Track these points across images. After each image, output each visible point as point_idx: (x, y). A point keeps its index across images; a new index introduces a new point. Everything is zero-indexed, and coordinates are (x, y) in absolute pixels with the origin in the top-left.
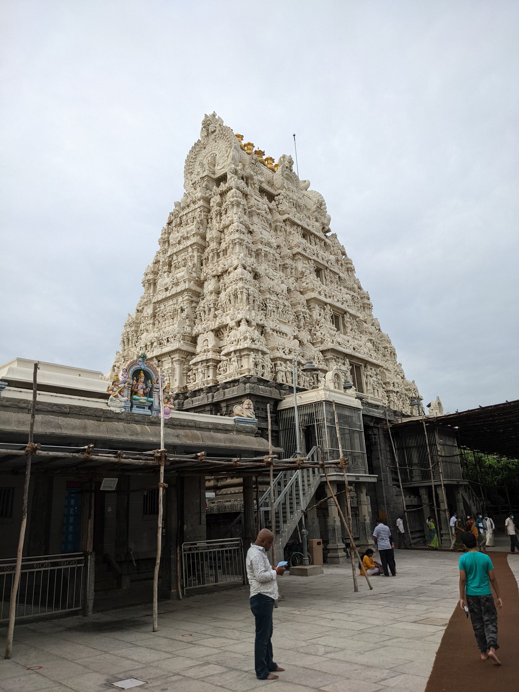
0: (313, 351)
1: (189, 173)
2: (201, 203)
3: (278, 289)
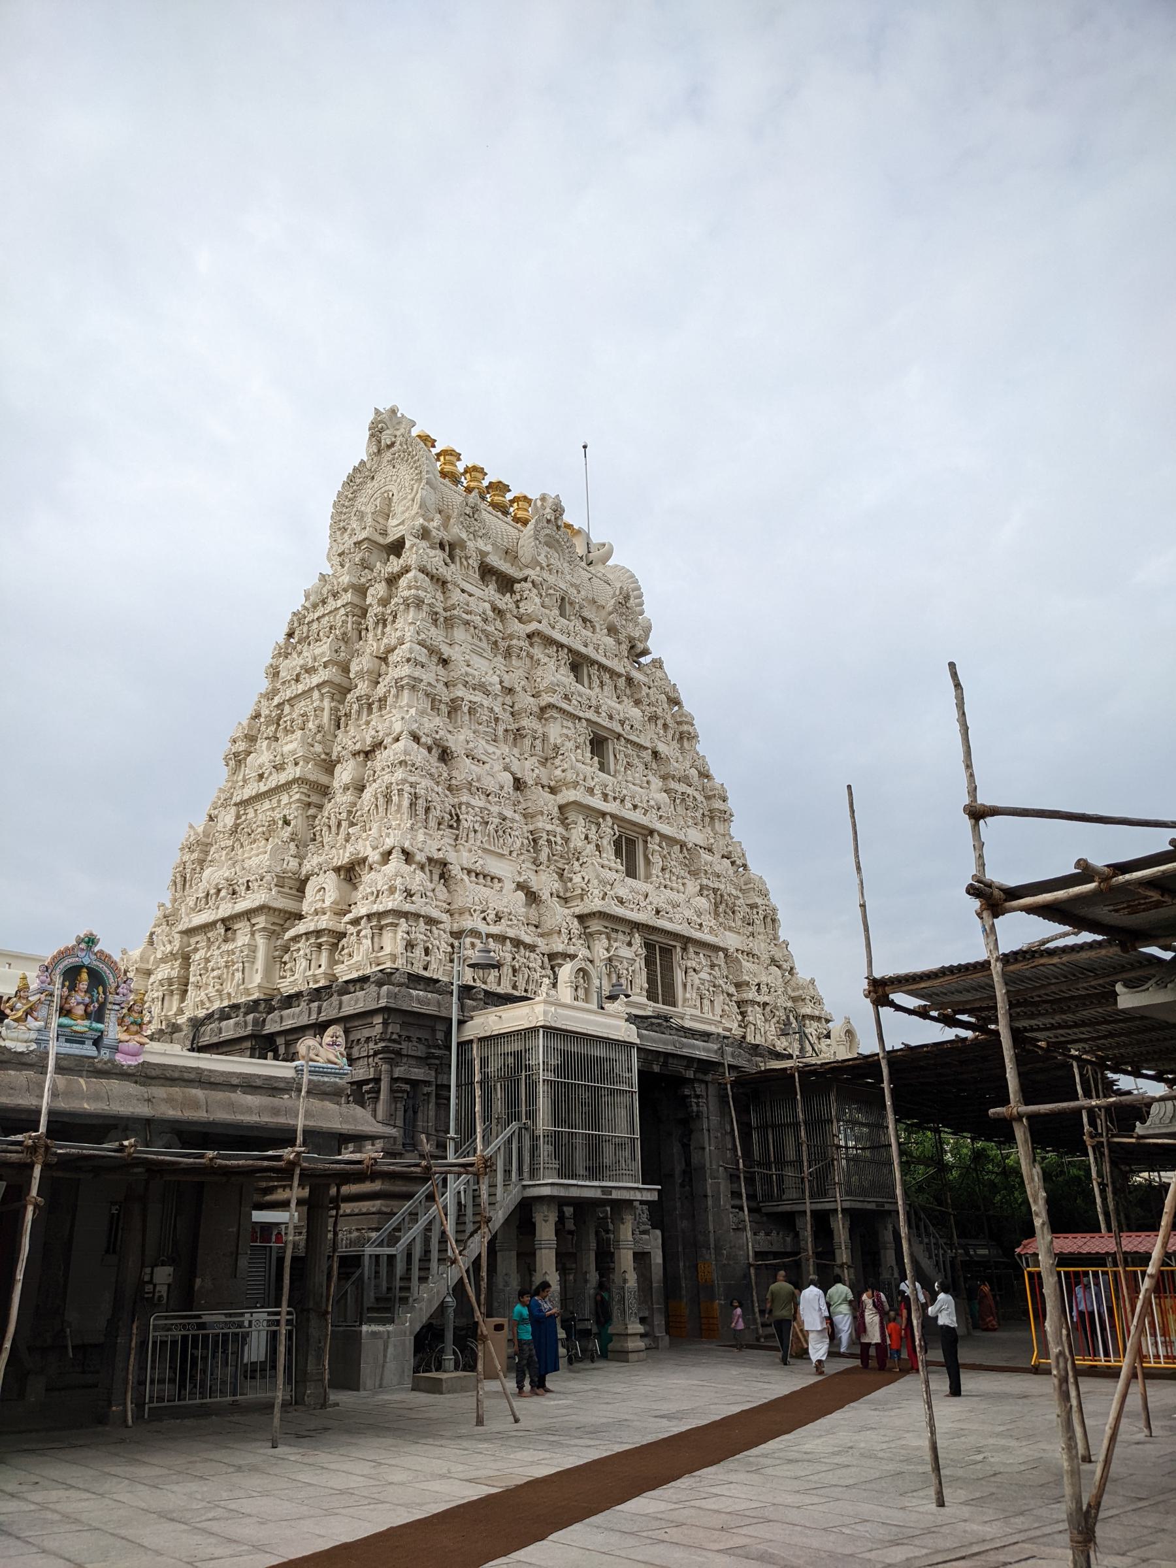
0: (559, 915)
1: (339, 529)
2: (348, 597)
3: (490, 784)
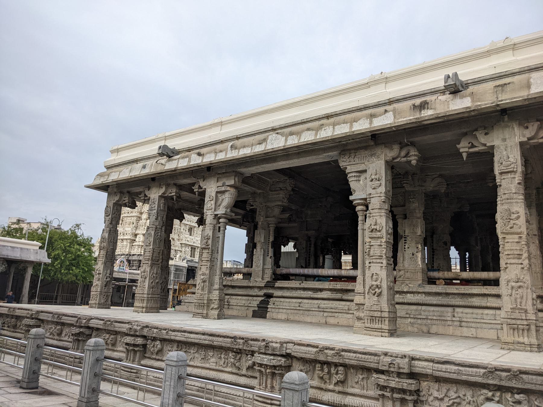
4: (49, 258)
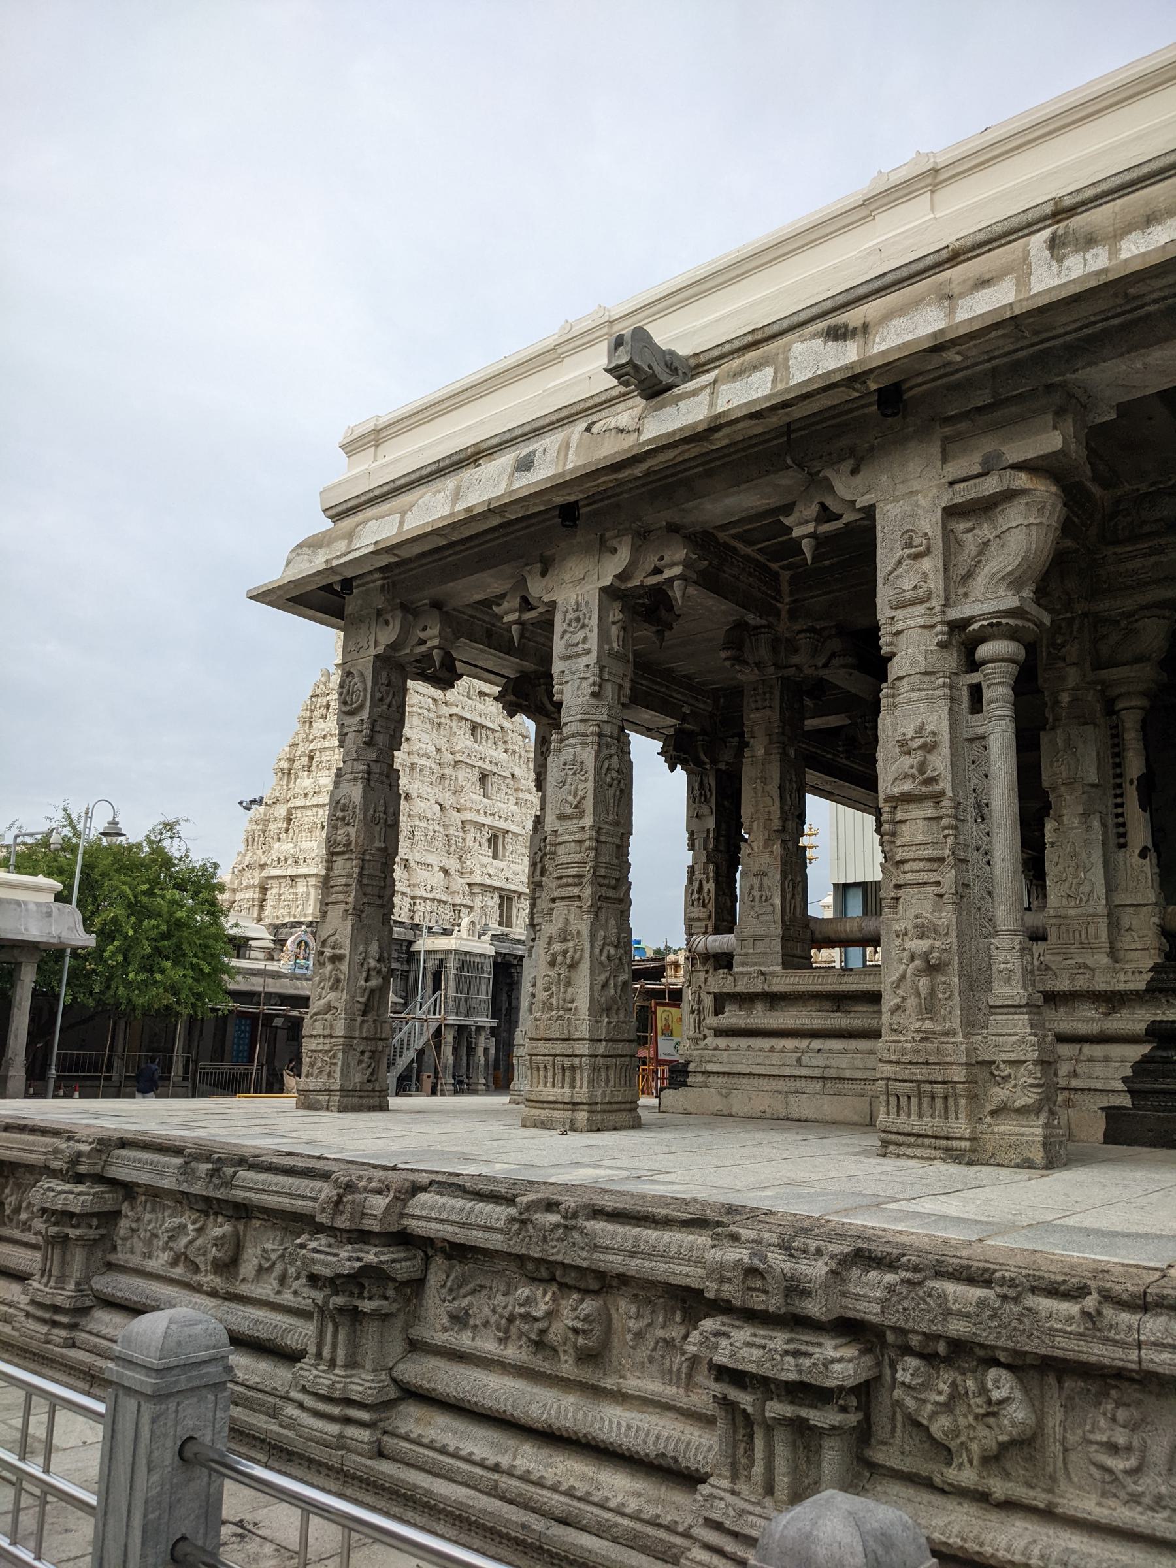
0: (460, 883)
4: (88, 930)
